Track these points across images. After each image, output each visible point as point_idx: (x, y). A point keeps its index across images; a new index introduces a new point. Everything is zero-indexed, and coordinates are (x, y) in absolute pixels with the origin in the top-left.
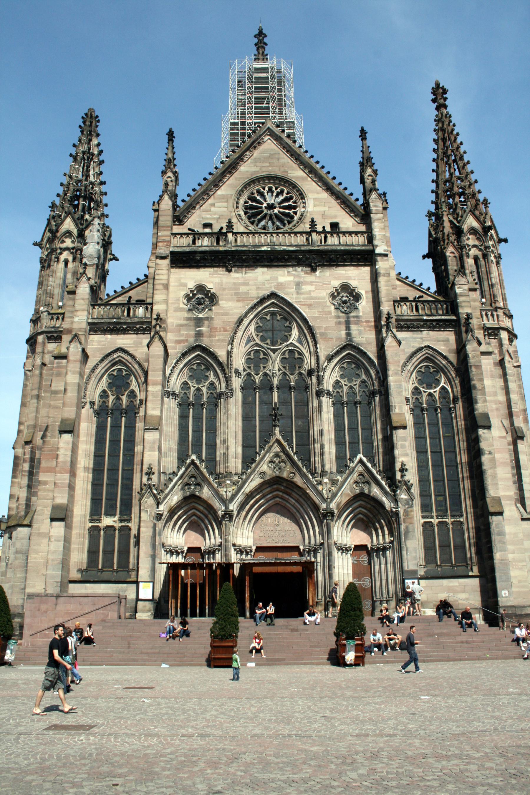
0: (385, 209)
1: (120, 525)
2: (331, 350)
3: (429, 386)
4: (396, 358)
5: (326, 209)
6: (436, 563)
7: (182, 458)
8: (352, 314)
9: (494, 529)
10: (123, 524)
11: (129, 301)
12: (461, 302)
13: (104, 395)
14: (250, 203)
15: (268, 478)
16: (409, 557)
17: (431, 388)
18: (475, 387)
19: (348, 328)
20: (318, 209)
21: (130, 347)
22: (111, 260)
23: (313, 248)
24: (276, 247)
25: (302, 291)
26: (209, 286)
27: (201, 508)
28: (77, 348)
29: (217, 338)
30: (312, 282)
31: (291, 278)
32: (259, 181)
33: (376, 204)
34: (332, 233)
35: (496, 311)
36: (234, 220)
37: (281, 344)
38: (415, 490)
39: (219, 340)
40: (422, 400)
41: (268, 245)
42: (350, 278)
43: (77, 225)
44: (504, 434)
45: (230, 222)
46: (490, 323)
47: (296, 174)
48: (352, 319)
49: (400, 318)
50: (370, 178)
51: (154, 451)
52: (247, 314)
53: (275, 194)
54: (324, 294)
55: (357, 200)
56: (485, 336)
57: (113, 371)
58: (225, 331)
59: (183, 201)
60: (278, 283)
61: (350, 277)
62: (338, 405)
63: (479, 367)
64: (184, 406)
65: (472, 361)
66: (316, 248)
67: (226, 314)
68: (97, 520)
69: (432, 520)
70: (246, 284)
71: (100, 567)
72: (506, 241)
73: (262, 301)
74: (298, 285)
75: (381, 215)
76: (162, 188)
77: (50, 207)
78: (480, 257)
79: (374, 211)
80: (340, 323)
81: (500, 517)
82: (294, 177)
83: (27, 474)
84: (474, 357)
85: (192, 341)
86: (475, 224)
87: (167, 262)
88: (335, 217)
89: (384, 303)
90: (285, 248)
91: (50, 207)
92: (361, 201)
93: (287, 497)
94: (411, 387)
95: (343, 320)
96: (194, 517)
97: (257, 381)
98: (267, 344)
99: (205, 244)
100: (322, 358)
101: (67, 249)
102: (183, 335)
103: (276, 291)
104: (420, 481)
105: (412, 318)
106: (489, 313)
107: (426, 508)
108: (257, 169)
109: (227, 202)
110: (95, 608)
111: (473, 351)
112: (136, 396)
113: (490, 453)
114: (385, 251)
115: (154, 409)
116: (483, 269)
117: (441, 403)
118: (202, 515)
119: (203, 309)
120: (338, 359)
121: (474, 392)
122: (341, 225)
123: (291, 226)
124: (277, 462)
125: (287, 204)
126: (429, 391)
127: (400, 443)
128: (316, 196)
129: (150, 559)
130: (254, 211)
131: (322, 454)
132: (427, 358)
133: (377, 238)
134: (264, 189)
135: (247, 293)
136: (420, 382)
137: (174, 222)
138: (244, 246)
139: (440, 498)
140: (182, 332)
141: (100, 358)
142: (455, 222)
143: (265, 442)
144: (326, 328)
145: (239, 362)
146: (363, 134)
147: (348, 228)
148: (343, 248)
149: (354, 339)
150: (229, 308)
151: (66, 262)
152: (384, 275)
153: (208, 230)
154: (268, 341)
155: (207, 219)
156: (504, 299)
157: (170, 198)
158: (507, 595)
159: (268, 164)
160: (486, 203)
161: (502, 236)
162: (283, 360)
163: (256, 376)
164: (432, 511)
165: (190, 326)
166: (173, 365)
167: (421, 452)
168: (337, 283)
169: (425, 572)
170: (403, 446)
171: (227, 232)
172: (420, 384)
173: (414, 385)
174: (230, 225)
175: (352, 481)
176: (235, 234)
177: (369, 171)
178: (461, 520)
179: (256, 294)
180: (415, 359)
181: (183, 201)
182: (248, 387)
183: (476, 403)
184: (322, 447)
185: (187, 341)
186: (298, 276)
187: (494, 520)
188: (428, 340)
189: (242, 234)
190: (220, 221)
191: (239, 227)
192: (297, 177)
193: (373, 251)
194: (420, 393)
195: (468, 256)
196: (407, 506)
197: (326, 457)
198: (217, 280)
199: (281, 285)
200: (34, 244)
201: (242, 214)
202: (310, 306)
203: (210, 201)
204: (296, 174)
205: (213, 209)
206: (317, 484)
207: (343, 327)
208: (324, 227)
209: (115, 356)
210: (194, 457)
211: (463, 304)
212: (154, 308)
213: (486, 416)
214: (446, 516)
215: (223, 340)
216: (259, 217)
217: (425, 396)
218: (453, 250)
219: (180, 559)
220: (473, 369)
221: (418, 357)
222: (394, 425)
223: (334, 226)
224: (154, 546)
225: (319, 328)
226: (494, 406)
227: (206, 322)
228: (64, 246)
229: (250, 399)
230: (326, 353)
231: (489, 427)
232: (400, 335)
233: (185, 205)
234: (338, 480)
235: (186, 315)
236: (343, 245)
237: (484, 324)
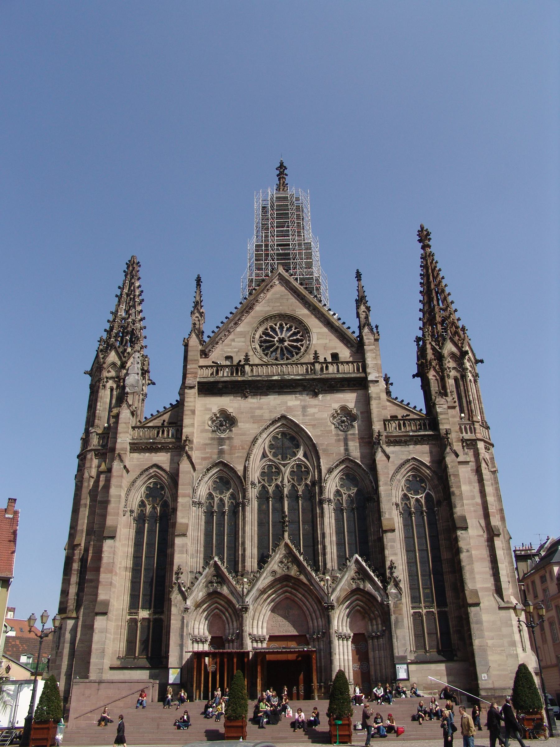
0: (377, 340)
1: (155, 617)
2: (332, 463)
3: (417, 493)
4: (386, 471)
5: (327, 341)
6: (425, 648)
7: (208, 558)
8: (349, 432)
9: (472, 618)
10: (157, 616)
11: (163, 424)
12: (441, 419)
13: (142, 504)
14: (265, 338)
15: (278, 576)
16: (399, 644)
18: (454, 494)
19: (346, 445)
20: (321, 341)
21: (163, 463)
22: (149, 384)
23: (316, 377)
24: (285, 377)
25: (307, 413)
26: (230, 410)
27: (223, 603)
28: (120, 465)
29: (236, 455)
30: (315, 405)
31: (298, 403)
32: (272, 319)
33: (368, 338)
34: (331, 363)
35: (474, 424)
36: (251, 353)
37: (290, 459)
38: (404, 585)
39: (238, 457)
40: (410, 505)
41: (279, 375)
42: (347, 401)
43: (120, 358)
44: (482, 533)
45: (247, 355)
46: (468, 436)
47: (302, 312)
48: (349, 437)
49: (390, 435)
50: (364, 313)
51: (183, 553)
52: (261, 433)
53: (285, 329)
54: (326, 415)
55: (354, 332)
56: (463, 447)
57: (150, 483)
58: (243, 449)
59: (209, 337)
60: (287, 407)
61: (348, 400)
62: (339, 511)
63: (457, 476)
64: (209, 514)
65: (451, 470)
66: (319, 377)
68: (135, 613)
69: (421, 610)
70: (260, 408)
71: (137, 655)
72: (482, 361)
73: (274, 422)
74: (304, 408)
75: (374, 346)
76: (191, 327)
77: (98, 341)
78: (459, 377)
79: (367, 344)
80: (339, 440)
81: (477, 608)
82: (300, 315)
83: (76, 573)
84: (452, 467)
85: (215, 458)
86: (454, 349)
87: (195, 390)
88: (335, 348)
89: (375, 423)
90: (293, 377)
91: (98, 341)
92: (357, 334)
93: (295, 592)
94: (401, 494)
95: (342, 438)
96: (216, 610)
97: (270, 491)
98: (279, 459)
99: (225, 375)
100: (324, 471)
101: (112, 378)
102: (208, 453)
103: (286, 414)
104: (409, 576)
105: (400, 434)
106: (468, 427)
107: (415, 599)
108: (270, 308)
109: (245, 337)
110: (131, 692)
111: (452, 462)
112: (168, 506)
113: (468, 551)
114: (376, 377)
115: (183, 517)
116: (462, 388)
117: (426, 507)
118: (223, 609)
119: (225, 431)
120: (338, 471)
121: (453, 497)
122: (340, 356)
123: (298, 357)
124: (286, 562)
125: (295, 338)
126: (416, 497)
127: (389, 544)
128: (319, 330)
129: (179, 647)
130: (267, 344)
131: (324, 554)
132: (413, 468)
133: (370, 366)
134: (276, 325)
136: (409, 489)
137: (201, 355)
138: (259, 376)
139: (427, 591)
140: (207, 451)
141: (139, 473)
142: (437, 347)
143: (276, 546)
144: (327, 445)
145: (255, 475)
146: (359, 276)
147: (345, 358)
148: (341, 376)
149: (352, 454)
150: (246, 428)
151: (112, 389)
152: (375, 399)
153: (228, 363)
154: (280, 457)
155: (229, 352)
156: (482, 413)
157: (197, 336)
158: (486, 678)
159: (279, 304)
160: (463, 329)
161: (478, 358)
162: (292, 473)
163: (269, 487)
164: (420, 602)
165: (214, 445)
166: (200, 478)
167: (410, 550)
169: (416, 657)
170: (392, 547)
171: (245, 364)
172: (408, 491)
173: (403, 492)
174: (247, 359)
175: (349, 578)
176: (251, 365)
177: (363, 308)
178: (446, 609)
179: (269, 416)
180: (403, 470)
181: (209, 337)
182: (263, 497)
183: (455, 507)
184: (324, 548)
185: (211, 457)
186: (304, 400)
187: (472, 610)
188: (414, 453)
189: (257, 365)
190: (239, 354)
191: (254, 360)
192: (303, 315)
193: (366, 378)
194: (408, 499)
195: (448, 376)
196: (396, 599)
197: (328, 557)
199: (290, 409)
200: (85, 373)
201: (258, 347)
202: (314, 426)
203: (231, 337)
204: (302, 312)
205: (233, 343)
206: (320, 581)
207: (342, 444)
208: (325, 358)
209: (151, 471)
210: (216, 559)
211: (443, 421)
212: (183, 431)
213: (464, 519)
214: (432, 607)
215: (241, 457)
216: (271, 350)
217: (413, 502)
218: (435, 374)
219: (206, 647)
220: (452, 478)
221: (406, 467)
222: (384, 529)
223: (335, 356)
224: (182, 636)
225: (322, 444)
226: (472, 509)
227: (227, 442)
228: (110, 375)
229: (264, 507)
230: (328, 466)
231: (466, 528)
232: (388, 450)
233: (210, 341)
234: (338, 577)
235: (210, 435)
236: (341, 373)
237: (463, 437)
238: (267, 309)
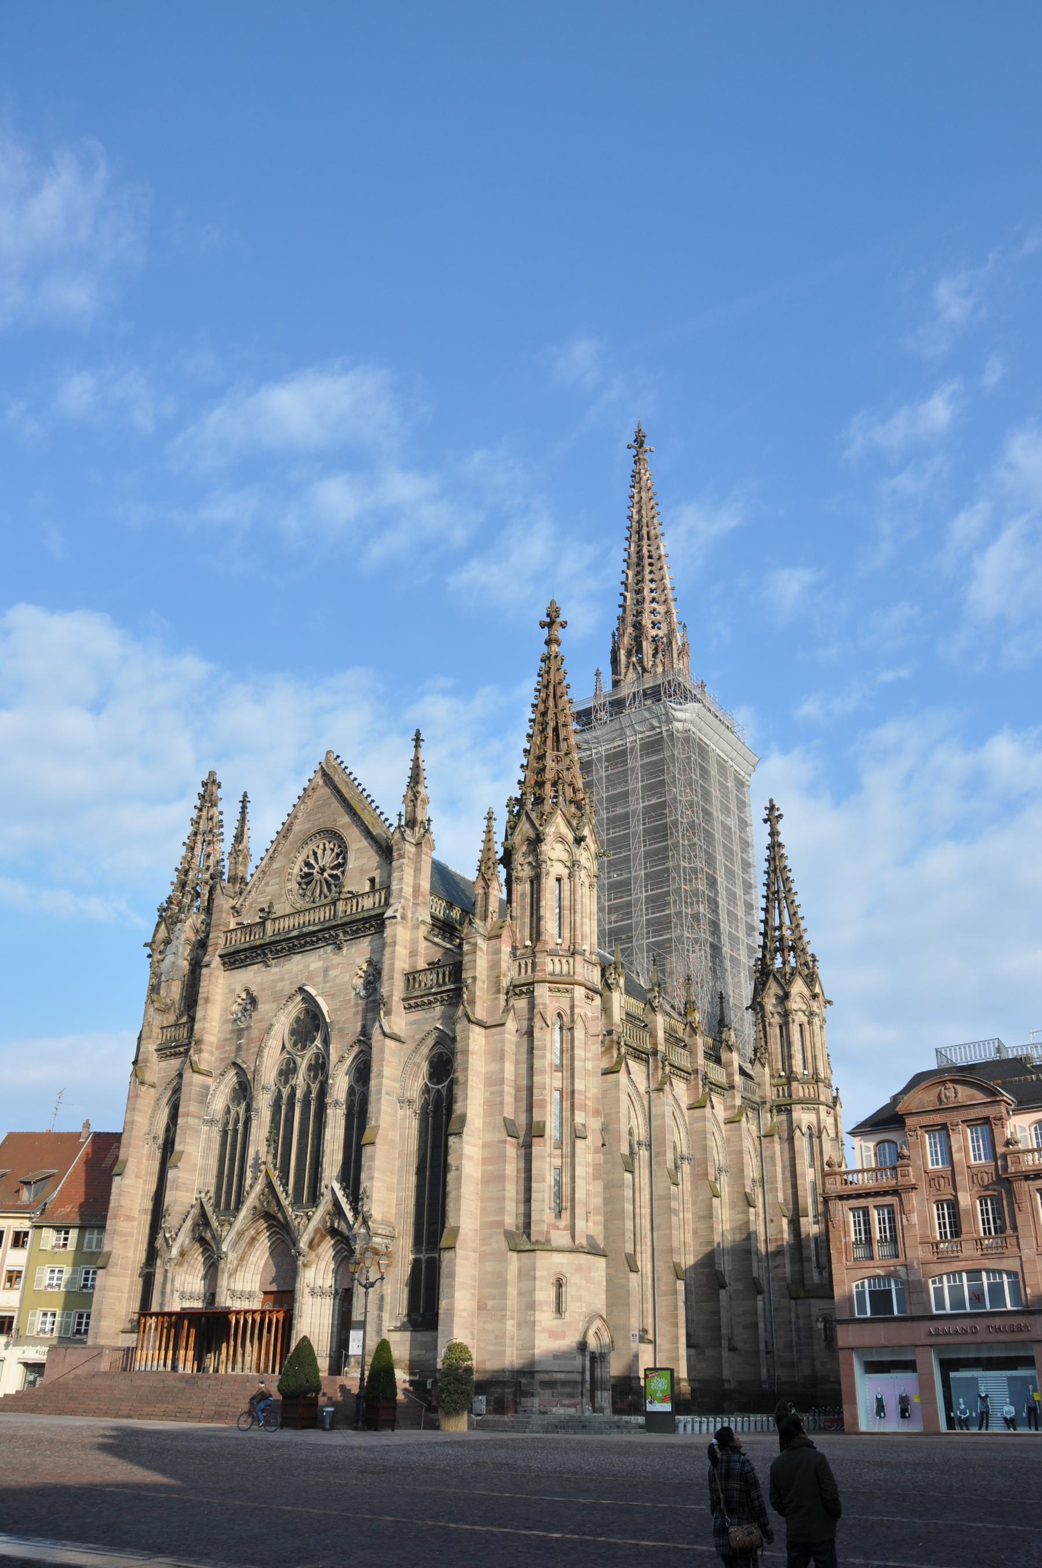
17: (439, 1083)
31: (320, 964)
67: (262, 1020)
70: (282, 980)
74: (326, 970)
84: (461, 1040)
135: (282, 991)
144: (345, 1022)
146: (418, 739)
155: (261, 903)
159: (319, 816)
183: (456, 1102)
198: (258, 980)
199: (311, 977)
205: (268, 889)
220: (459, 1057)
225: (338, 1022)
227: (246, 1032)
238: (307, 826)
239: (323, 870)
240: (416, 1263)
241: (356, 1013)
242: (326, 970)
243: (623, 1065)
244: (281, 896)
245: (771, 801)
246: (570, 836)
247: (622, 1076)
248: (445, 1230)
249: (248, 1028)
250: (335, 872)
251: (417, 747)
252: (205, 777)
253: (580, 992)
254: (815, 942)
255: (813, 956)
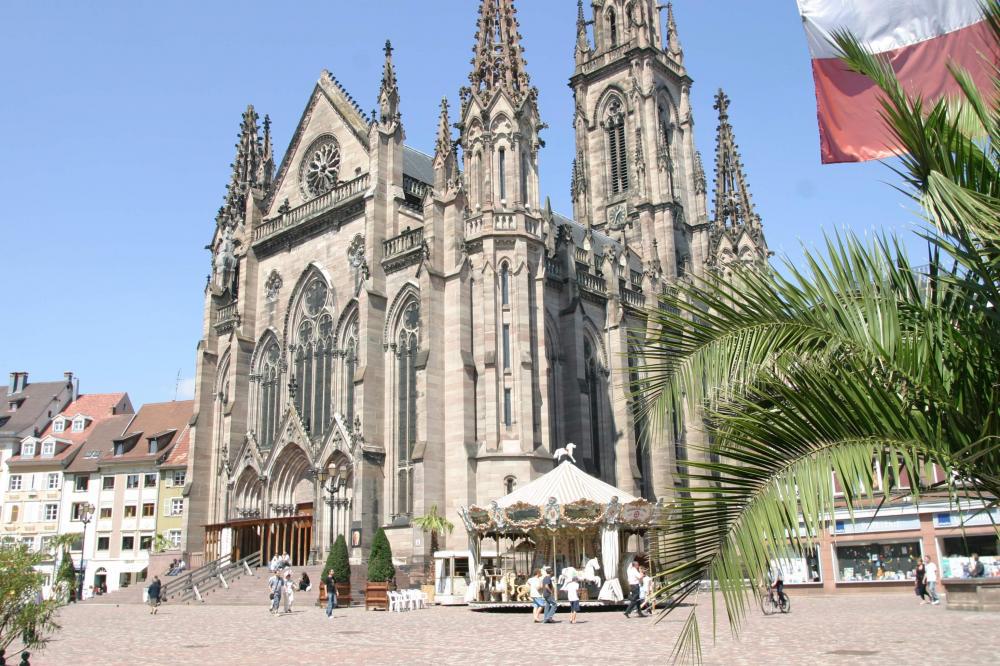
25: (331, 253)
26: (279, 270)
67: (286, 294)
70: (298, 260)
74: (328, 248)
78: (482, 151)
88: (359, 161)
135: (298, 269)
136: (407, 323)
146: (388, 49)
168: (352, 237)
182: (299, 361)
199: (318, 255)
205: (286, 189)
239: (324, 168)
240: (402, 474)
241: (351, 279)
242: (328, 248)
243: (578, 307)
244: (295, 194)
245: (720, 90)
246: (510, 112)
247: (578, 316)
248: (416, 446)
249: (277, 301)
250: (332, 169)
251: (388, 54)
252: (245, 110)
253: (521, 245)
254: (759, 203)
255: (757, 216)
